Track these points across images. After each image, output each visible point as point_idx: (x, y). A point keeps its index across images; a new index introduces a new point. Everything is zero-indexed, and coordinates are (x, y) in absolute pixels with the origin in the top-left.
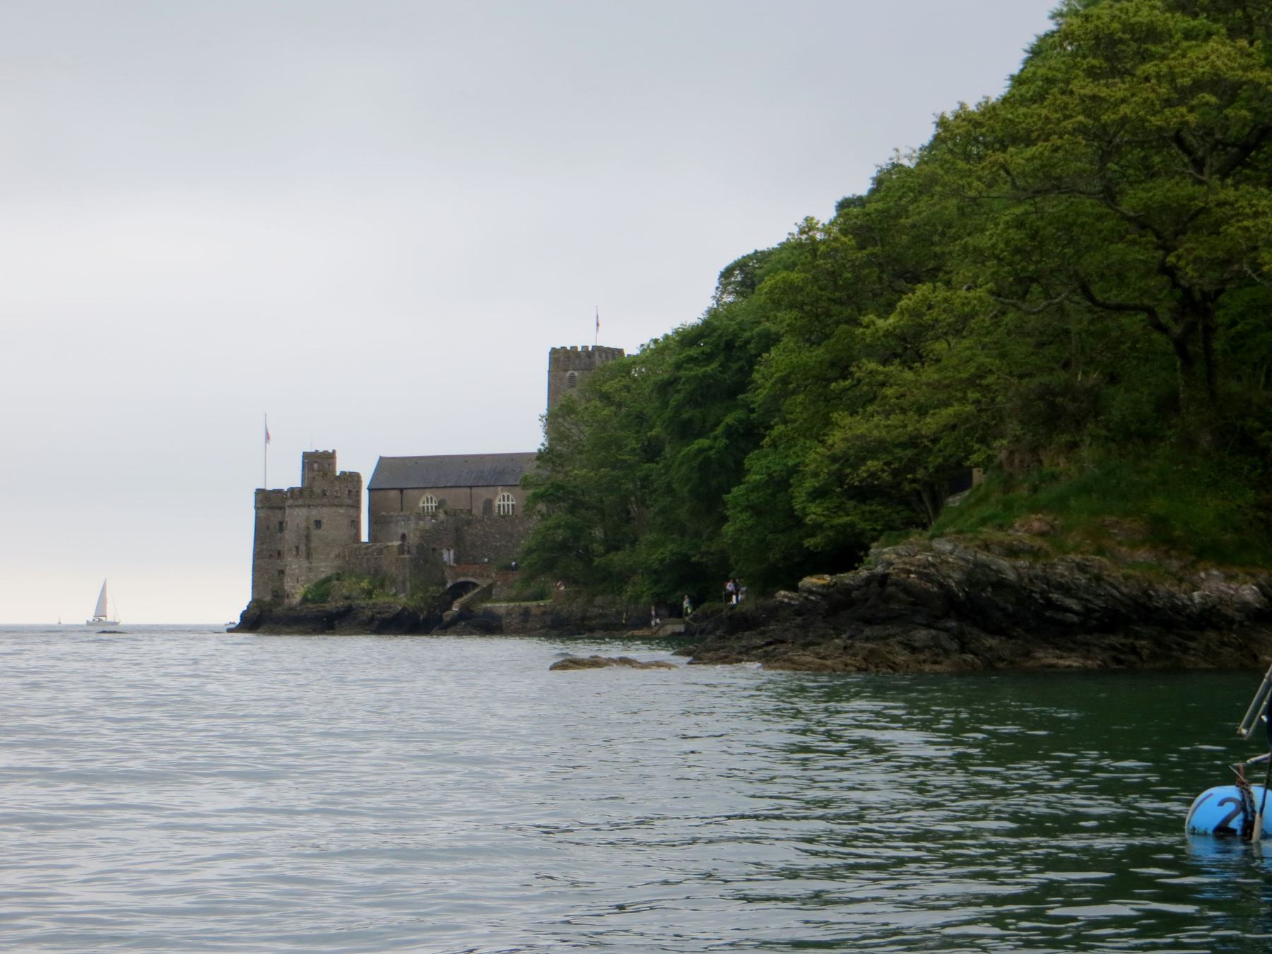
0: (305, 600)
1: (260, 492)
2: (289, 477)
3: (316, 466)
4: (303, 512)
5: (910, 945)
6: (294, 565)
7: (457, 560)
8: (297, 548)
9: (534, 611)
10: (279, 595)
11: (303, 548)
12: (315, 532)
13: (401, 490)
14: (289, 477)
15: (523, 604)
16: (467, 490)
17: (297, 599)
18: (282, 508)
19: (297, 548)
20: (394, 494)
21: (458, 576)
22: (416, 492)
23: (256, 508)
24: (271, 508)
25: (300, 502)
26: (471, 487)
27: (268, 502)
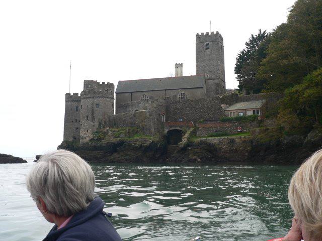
0: (92, 140)
1: (68, 95)
2: (79, 89)
3: (89, 86)
4: (91, 101)
5: (237, 238)
6: (85, 124)
7: (167, 120)
8: (87, 117)
9: (237, 141)
10: (76, 138)
11: (90, 116)
12: (95, 109)
13: (131, 93)
14: (79, 89)
15: (229, 137)
16: (164, 92)
17: (88, 139)
18: (80, 101)
19: (87, 117)
20: (127, 95)
21: (171, 127)
22: (139, 94)
23: (66, 101)
24: (73, 101)
25: (89, 96)
26: (166, 90)
27: (71, 99)
